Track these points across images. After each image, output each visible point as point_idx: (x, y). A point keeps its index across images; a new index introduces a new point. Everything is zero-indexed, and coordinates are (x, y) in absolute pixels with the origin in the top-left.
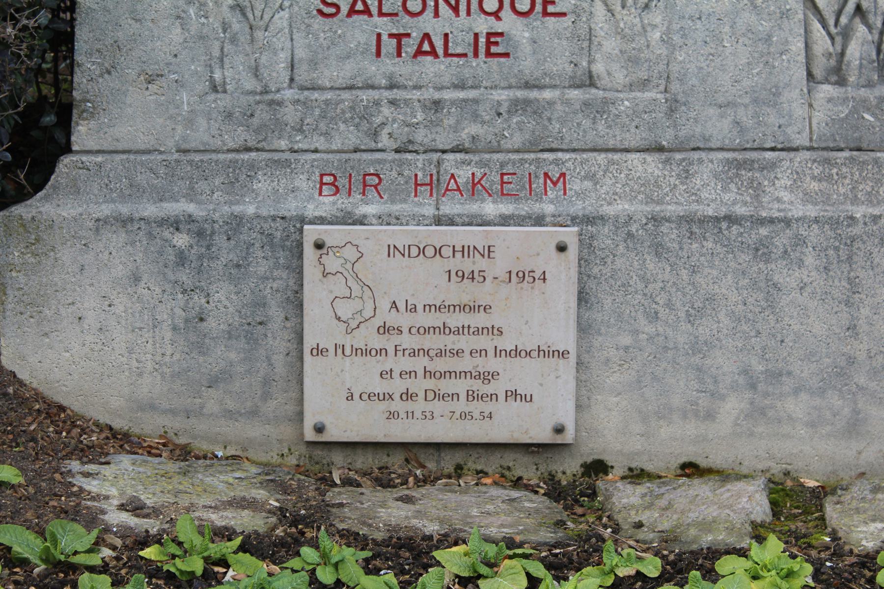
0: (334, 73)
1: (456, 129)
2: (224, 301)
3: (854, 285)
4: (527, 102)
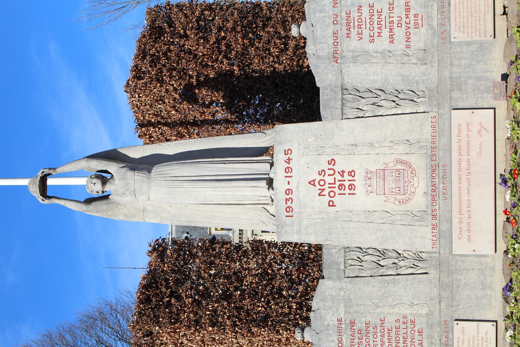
1: (436, 340)
4: (431, 326)
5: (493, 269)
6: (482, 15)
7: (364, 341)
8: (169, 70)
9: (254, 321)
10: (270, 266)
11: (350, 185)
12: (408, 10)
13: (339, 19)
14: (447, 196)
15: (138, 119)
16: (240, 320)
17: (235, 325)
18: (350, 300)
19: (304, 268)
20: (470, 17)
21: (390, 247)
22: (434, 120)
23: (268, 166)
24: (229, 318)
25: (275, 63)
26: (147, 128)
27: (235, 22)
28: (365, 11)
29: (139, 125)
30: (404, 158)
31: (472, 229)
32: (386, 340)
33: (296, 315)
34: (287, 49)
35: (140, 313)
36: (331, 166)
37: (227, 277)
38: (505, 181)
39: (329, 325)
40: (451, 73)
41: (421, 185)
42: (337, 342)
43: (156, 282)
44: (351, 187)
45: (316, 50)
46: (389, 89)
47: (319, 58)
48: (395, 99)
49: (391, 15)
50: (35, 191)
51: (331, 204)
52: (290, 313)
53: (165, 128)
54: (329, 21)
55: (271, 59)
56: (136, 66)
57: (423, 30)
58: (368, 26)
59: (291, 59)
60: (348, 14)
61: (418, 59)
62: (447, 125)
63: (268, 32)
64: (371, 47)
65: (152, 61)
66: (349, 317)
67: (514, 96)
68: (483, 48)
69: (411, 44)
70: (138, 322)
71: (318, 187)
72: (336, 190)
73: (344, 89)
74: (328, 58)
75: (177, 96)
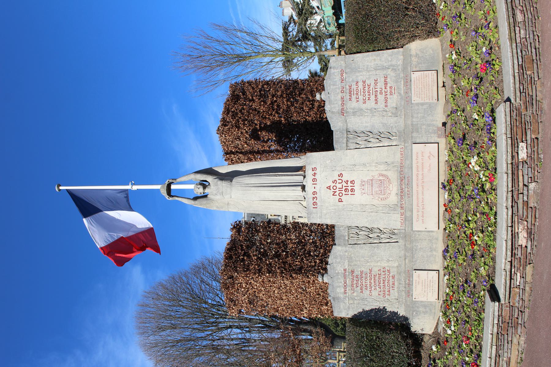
0: (396, 294)
2: (421, 309)
3: (420, 239)
5: (437, 239)
6: (430, 87)
7: (359, 282)
8: (243, 121)
9: (294, 270)
10: (304, 237)
11: (352, 189)
12: (386, 84)
13: (344, 89)
14: (410, 195)
15: (224, 150)
16: (285, 269)
17: (282, 272)
18: (351, 258)
19: (324, 239)
20: (423, 89)
21: (376, 227)
22: (402, 150)
23: (302, 177)
24: (279, 268)
25: (307, 116)
26: (231, 155)
27: (282, 92)
28: (360, 85)
29: (225, 153)
30: (384, 173)
31: (424, 215)
32: (372, 281)
33: (319, 266)
34: (313, 108)
35: (226, 265)
36: (340, 178)
37: (277, 244)
38: (444, 187)
39: (338, 273)
40: (412, 122)
41: (394, 189)
42: (343, 283)
43: (235, 247)
44: (352, 190)
45: (331, 108)
46: (375, 131)
47: (333, 113)
48: (379, 137)
49: (376, 87)
50: (164, 192)
51: (340, 201)
52: (315, 266)
53: (241, 155)
54: (339, 91)
55: (304, 114)
56: (224, 118)
57: (395, 96)
58: (362, 93)
59: (316, 114)
60: (350, 87)
61: (392, 113)
62: (410, 153)
63: (302, 98)
64: (364, 106)
65: (233, 115)
66: (351, 268)
67: (450, 135)
68: (431, 107)
69: (388, 104)
70: (224, 270)
71: (332, 190)
72: (343, 192)
73: (348, 131)
74: (338, 113)
75: (248, 136)
